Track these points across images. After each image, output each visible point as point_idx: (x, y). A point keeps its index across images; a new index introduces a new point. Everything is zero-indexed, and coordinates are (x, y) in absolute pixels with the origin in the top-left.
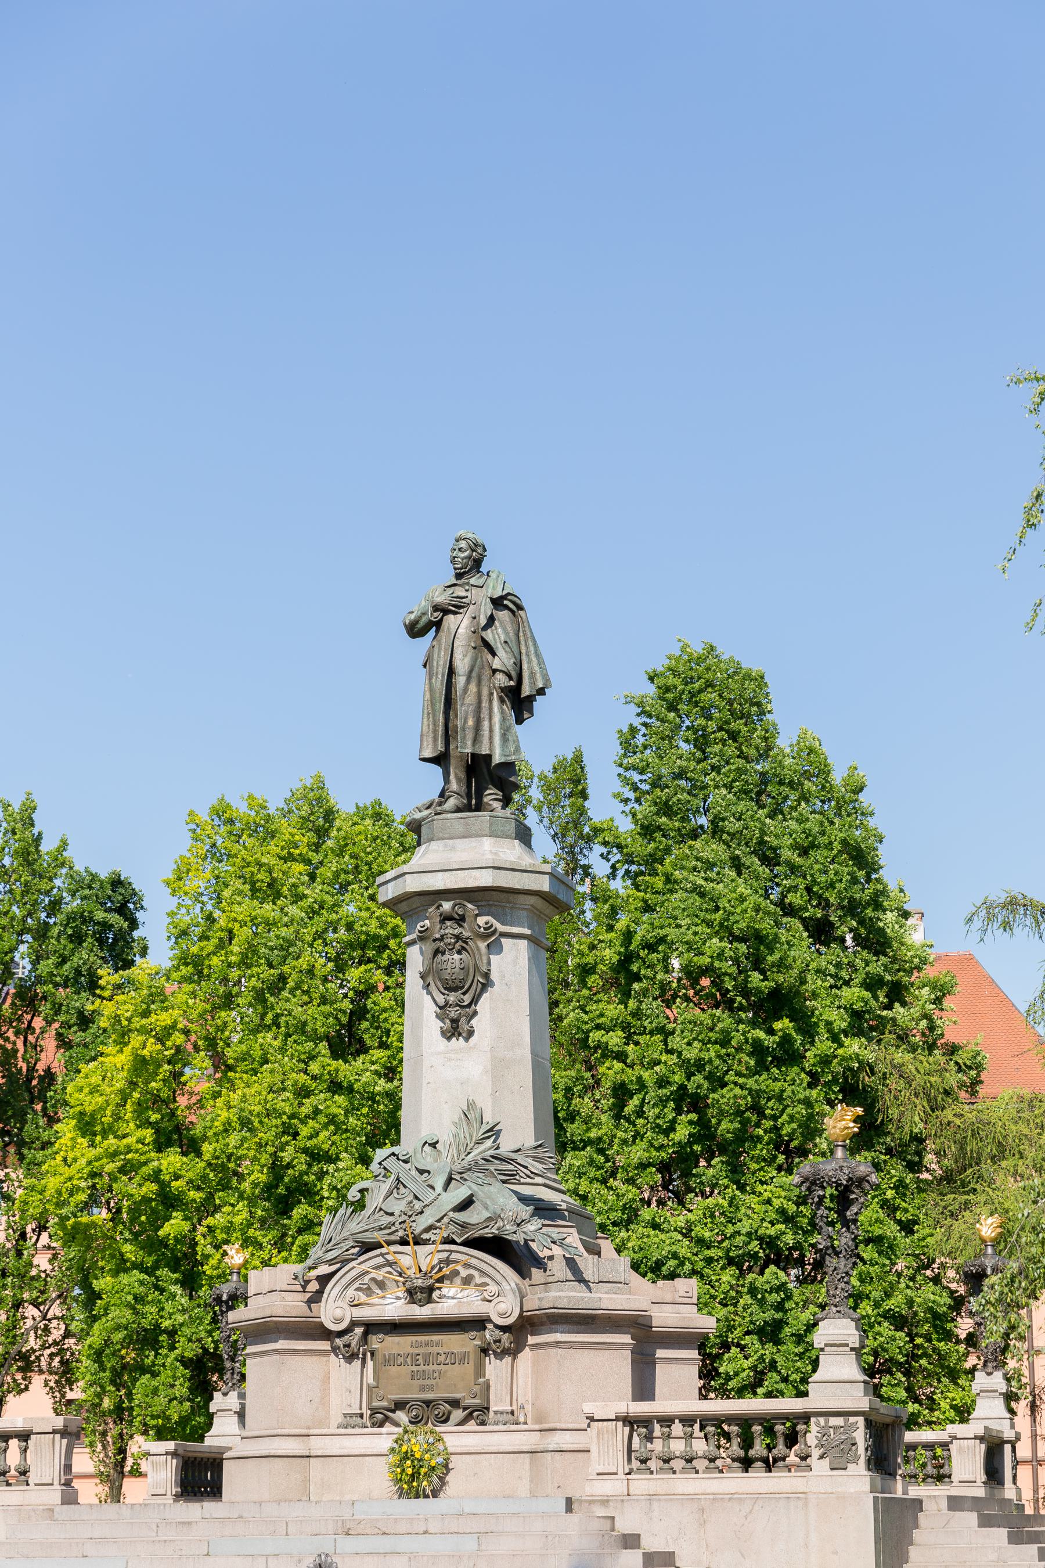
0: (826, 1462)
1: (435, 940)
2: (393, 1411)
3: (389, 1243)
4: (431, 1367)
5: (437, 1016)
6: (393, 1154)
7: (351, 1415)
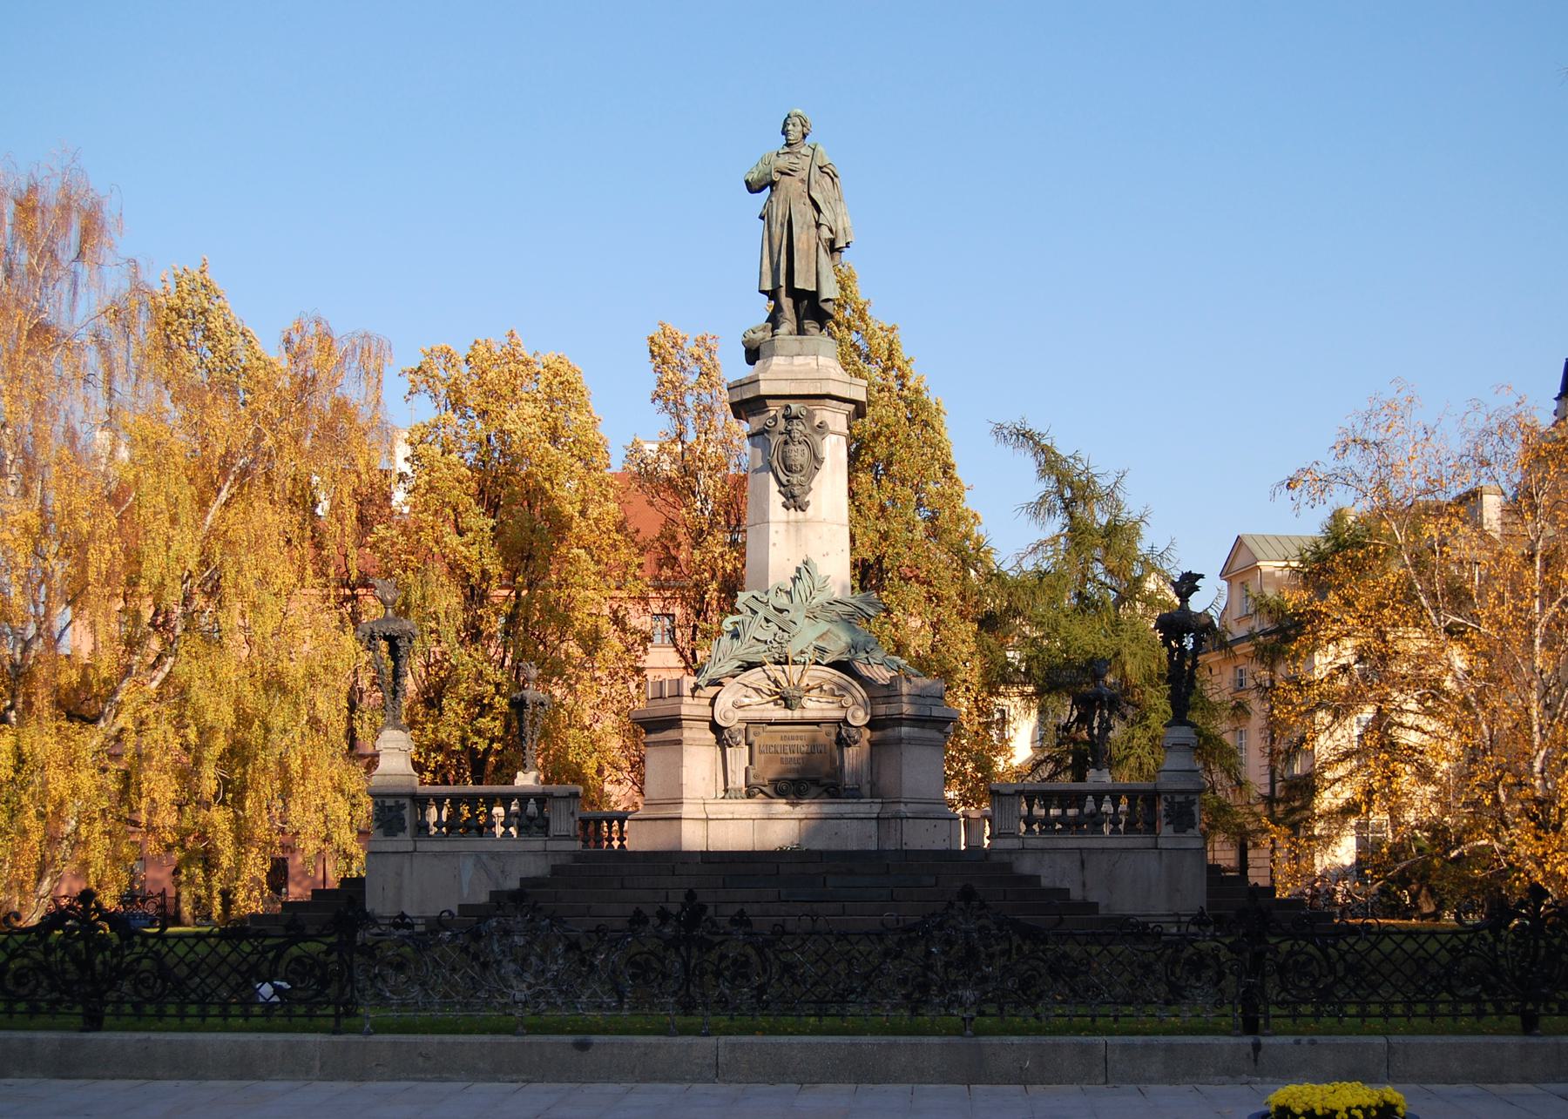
0: (1170, 828)
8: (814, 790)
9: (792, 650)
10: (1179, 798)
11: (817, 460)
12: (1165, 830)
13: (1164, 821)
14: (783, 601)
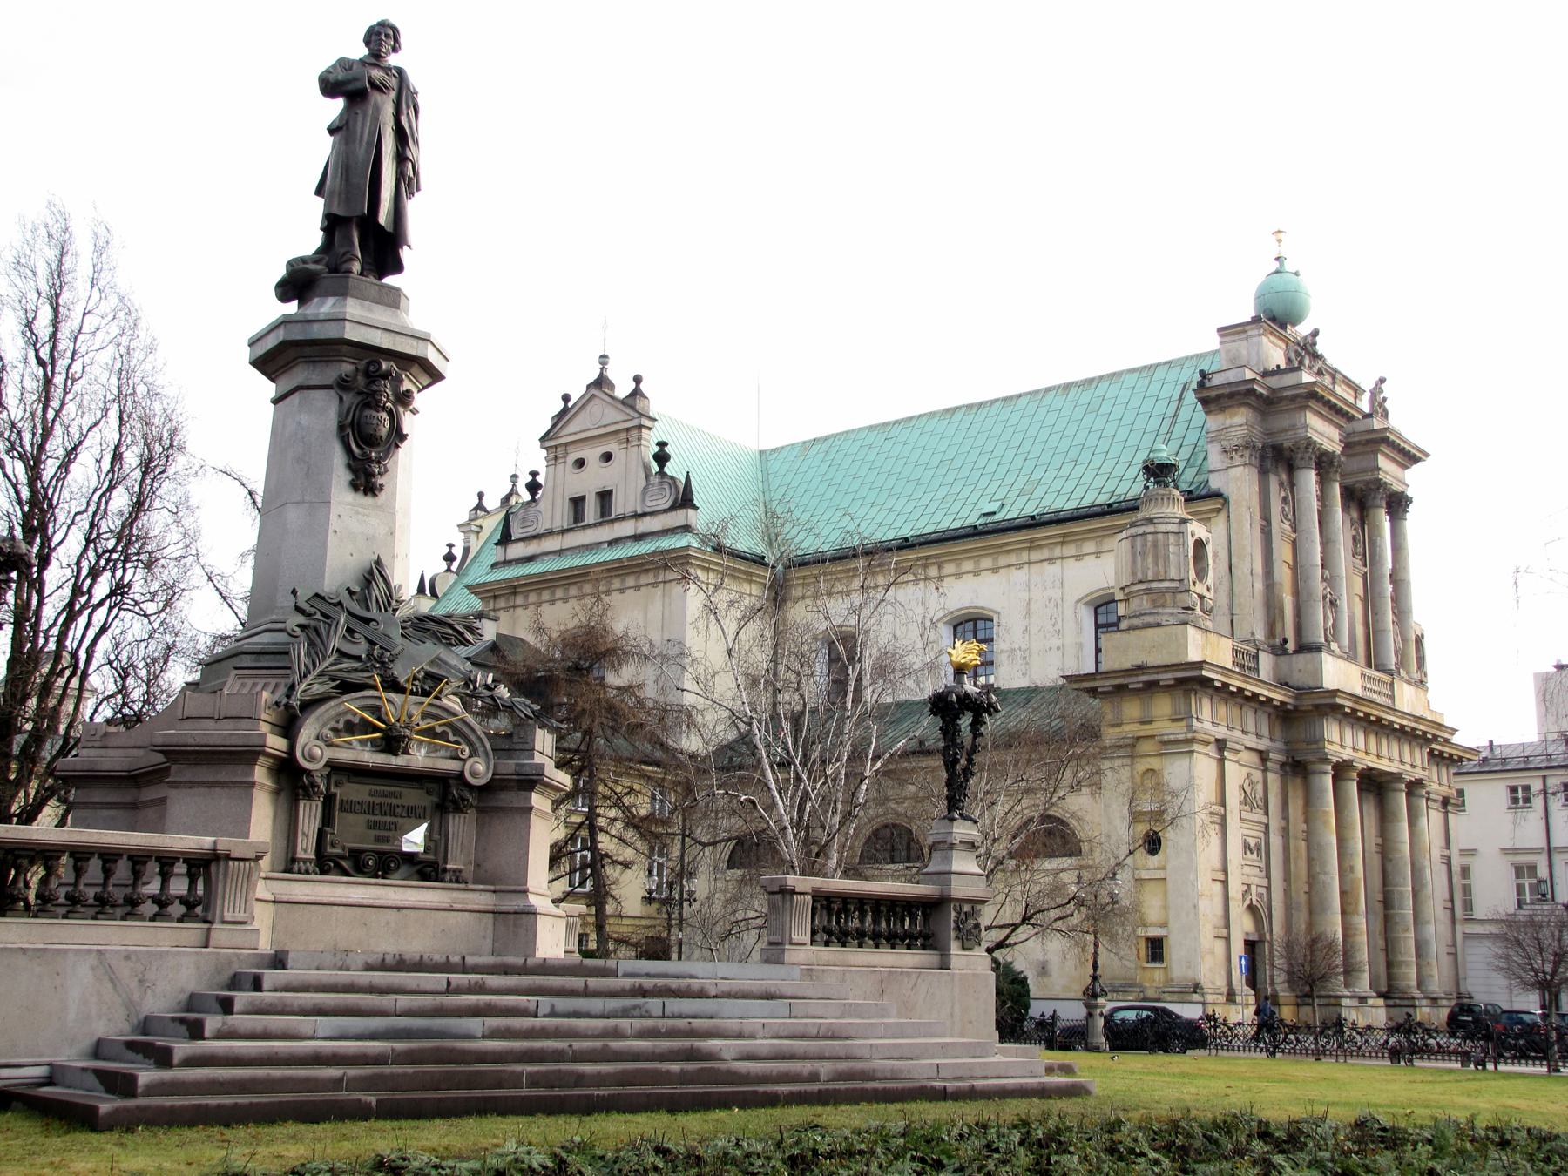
1: (360, 393)
2: (343, 858)
3: (385, 689)
4: (388, 819)
5: (349, 466)
6: (317, 595)
7: (305, 861)
8: (404, 869)
9: (402, 673)
10: (967, 908)
11: (398, 436)
12: (955, 948)
13: (953, 934)
14: (357, 609)
